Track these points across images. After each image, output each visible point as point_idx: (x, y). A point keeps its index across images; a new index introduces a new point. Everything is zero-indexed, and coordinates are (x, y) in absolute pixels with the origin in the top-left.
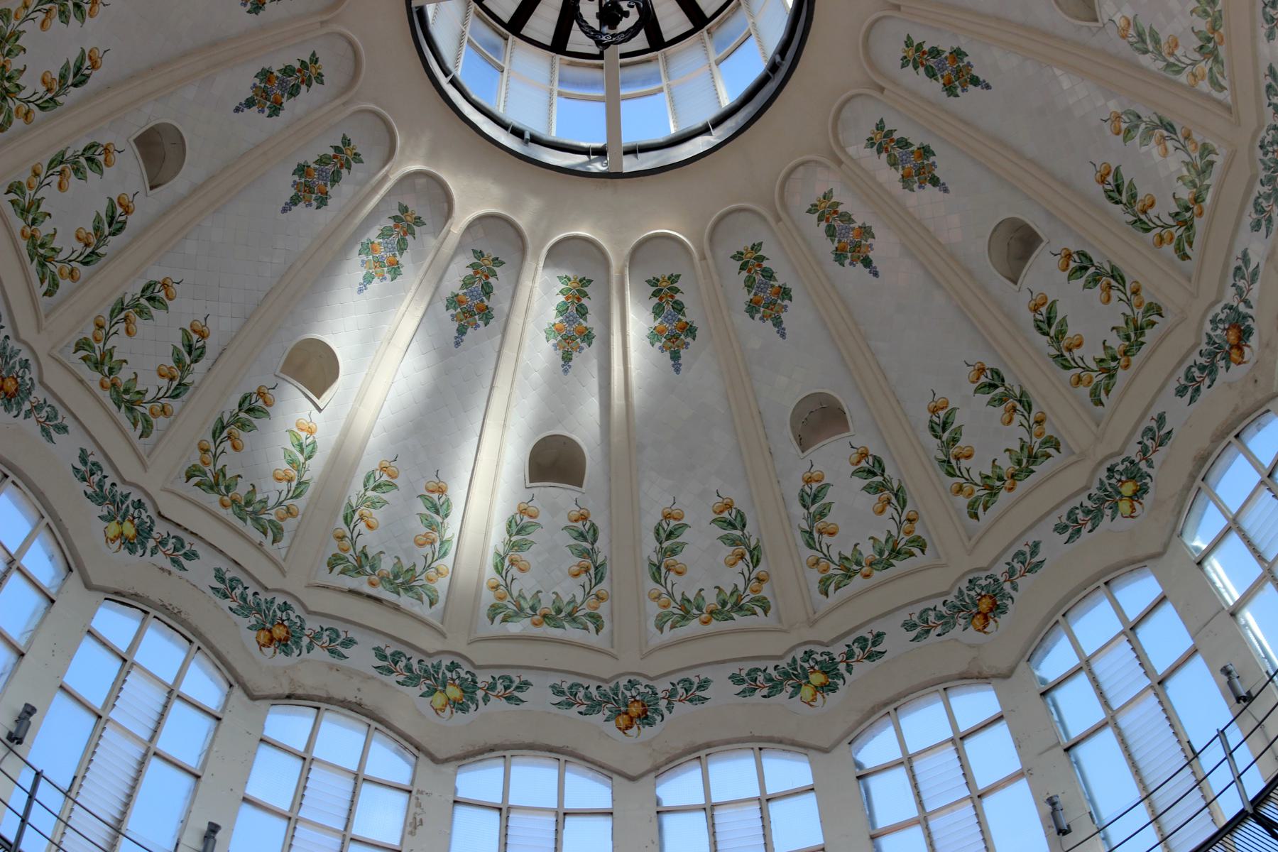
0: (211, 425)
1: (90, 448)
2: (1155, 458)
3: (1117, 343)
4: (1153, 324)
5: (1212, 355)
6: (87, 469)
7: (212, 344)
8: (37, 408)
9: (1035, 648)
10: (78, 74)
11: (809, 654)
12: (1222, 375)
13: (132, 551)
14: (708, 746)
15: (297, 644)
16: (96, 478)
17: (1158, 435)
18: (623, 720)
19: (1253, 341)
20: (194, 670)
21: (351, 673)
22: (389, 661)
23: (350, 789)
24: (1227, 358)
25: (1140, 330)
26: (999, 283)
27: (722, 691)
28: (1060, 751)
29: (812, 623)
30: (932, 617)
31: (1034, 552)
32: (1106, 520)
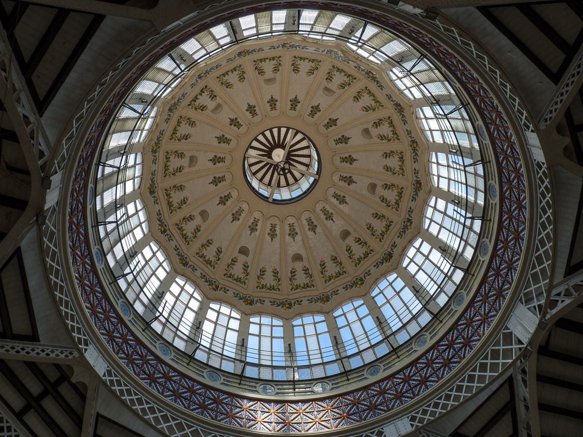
0: (183, 217)
1: (161, 210)
2: (367, 278)
3: (362, 256)
4: (371, 253)
5: (383, 260)
6: (159, 214)
7: (188, 202)
8: (155, 197)
9: (335, 309)
10: (186, 137)
11: (286, 301)
12: (384, 264)
13: (162, 234)
14: (263, 313)
15: (187, 266)
16: (160, 216)
17: (368, 273)
18: (246, 303)
19: (393, 258)
20: (165, 262)
21: (195, 276)
22: (203, 276)
23: (189, 299)
24: (386, 261)
25: (368, 254)
26: (340, 241)
27: (267, 303)
28: (337, 329)
29: (288, 295)
30: (313, 299)
31: (337, 292)
32: (354, 288)
